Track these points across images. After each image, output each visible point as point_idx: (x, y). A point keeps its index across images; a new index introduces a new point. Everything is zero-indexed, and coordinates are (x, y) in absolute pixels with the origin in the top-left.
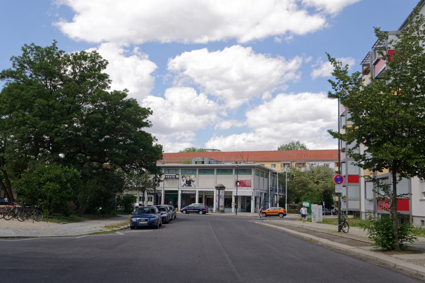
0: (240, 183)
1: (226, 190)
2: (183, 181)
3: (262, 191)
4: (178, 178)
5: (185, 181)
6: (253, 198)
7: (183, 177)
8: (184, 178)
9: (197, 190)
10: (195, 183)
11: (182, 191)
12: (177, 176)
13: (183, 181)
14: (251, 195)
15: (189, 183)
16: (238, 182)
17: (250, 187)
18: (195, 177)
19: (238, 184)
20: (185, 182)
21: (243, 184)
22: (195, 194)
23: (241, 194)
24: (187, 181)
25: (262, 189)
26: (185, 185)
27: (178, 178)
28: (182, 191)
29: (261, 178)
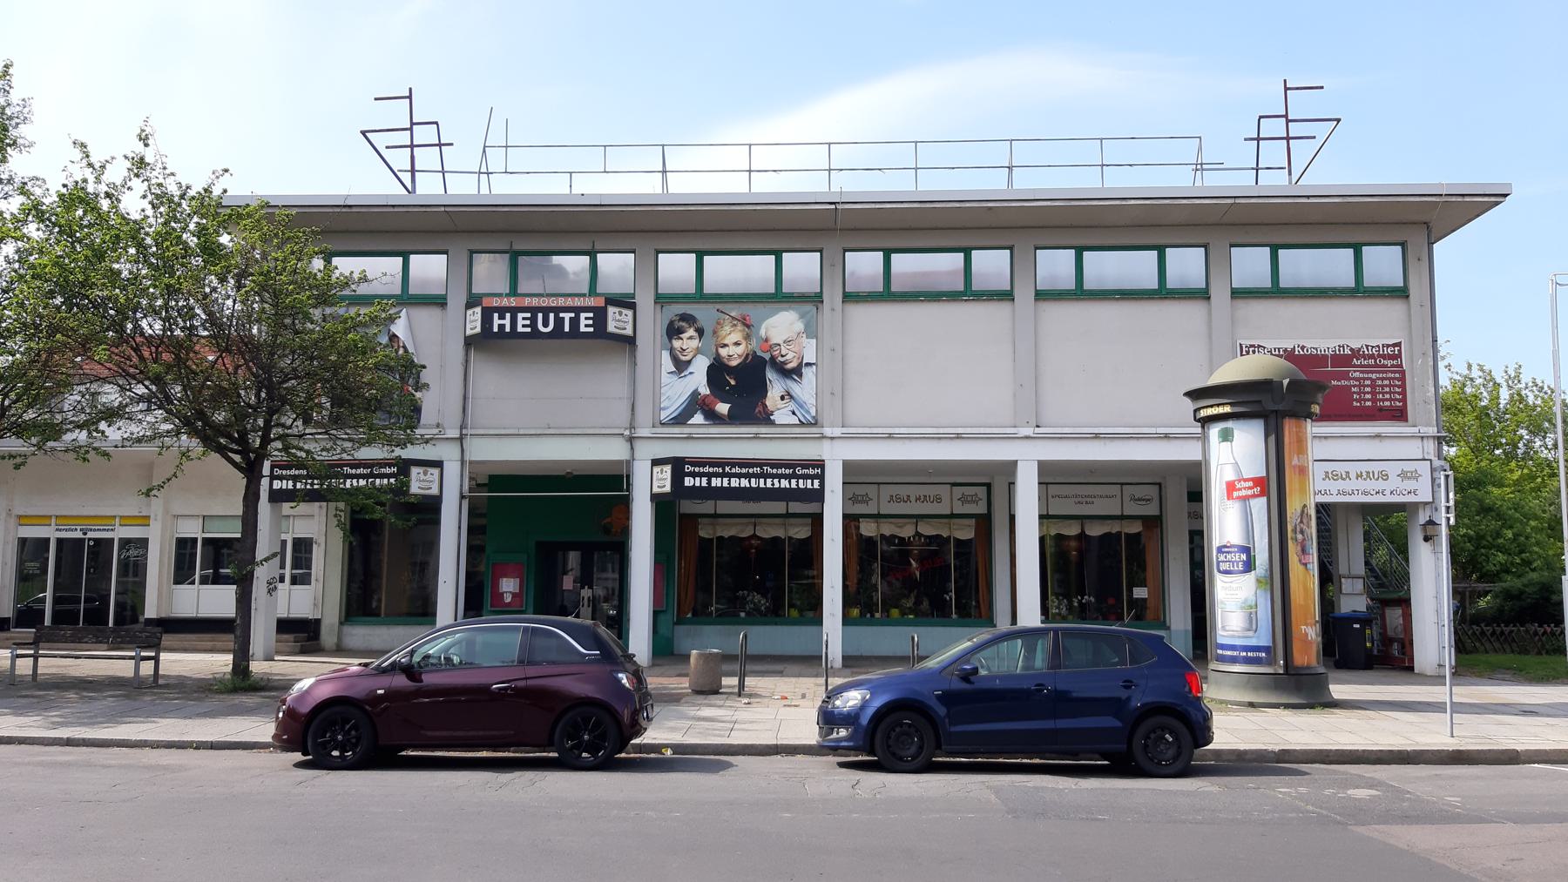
2: (681, 366)
4: (630, 341)
5: (701, 366)
7: (673, 332)
8: (688, 342)
9: (835, 457)
10: (805, 389)
13: (681, 366)
15: (742, 388)
17: (1399, 415)
18: (811, 331)
20: (697, 379)
22: (818, 496)
24: (717, 371)
26: (696, 403)
27: (630, 341)
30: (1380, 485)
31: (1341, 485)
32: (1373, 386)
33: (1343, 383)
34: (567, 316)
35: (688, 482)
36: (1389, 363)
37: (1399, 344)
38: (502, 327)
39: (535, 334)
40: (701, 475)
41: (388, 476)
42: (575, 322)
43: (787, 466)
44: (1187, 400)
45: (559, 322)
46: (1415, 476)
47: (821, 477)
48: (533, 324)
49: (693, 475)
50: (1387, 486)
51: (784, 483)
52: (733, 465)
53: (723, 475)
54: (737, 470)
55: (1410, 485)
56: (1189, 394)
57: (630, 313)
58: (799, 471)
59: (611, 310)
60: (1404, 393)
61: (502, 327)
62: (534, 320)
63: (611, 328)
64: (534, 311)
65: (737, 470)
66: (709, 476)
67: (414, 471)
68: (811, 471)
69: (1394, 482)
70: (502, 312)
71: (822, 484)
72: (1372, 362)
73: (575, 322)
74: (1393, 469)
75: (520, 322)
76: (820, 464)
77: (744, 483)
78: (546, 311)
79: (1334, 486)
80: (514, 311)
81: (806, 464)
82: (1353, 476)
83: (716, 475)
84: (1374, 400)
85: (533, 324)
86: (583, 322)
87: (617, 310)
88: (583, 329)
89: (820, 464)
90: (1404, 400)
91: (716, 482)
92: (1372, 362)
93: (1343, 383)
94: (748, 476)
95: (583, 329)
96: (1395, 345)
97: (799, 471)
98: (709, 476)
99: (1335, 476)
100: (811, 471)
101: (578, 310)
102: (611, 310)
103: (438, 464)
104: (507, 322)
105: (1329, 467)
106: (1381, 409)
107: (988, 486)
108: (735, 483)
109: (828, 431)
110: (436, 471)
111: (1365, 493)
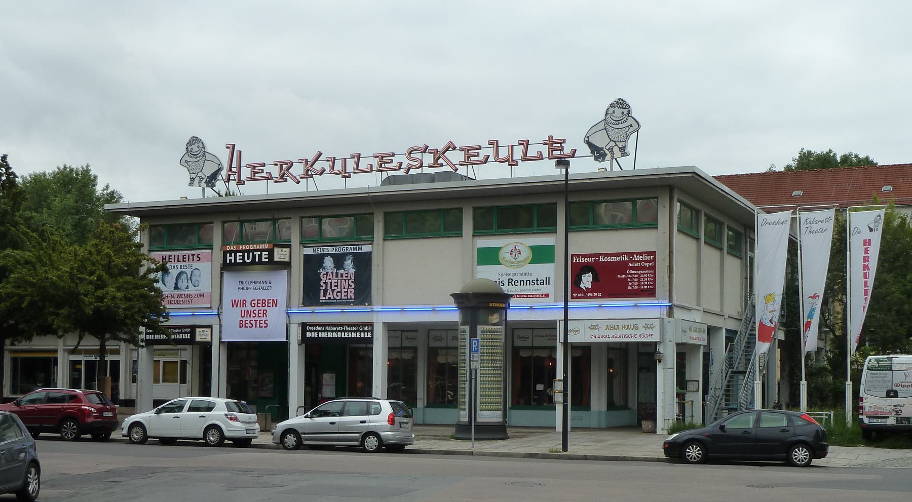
0: (595, 280)
1: (512, 316)
3: (715, 322)
6: (669, 354)
11: (304, 326)
12: (280, 255)
14: (656, 338)
16: (586, 268)
17: (651, 293)
19: (587, 280)
21: (611, 279)
22: (370, 341)
23: (602, 332)
25: (717, 309)
28: (304, 326)
29: (710, 255)
30: (633, 332)
31: (614, 332)
32: (639, 278)
33: (624, 276)
34: (257, 254)
35: (308, 335)
36: (647, 265)
37: (654, 253)
38: (230, 260)
39: (244, 263)
40: (314, 331)
41: (187, 333)
42: (260, 256)
43: (355, 326)
44: (452, 299)
45: (254, 256)
46: (652, 327)
47: (372, 331)
48: (243, 259)
49: (311, 331)
50: (638, 332)
51: (354, 335)
52: (329, 326)
53: (324, 331)
54: (331, 328)
55: (649, 332)
56: (452, 295)
57: (288, 250)
58: (361, 328)
59: (276, 250)
60: (655, 281)
61: (230, 260)
62: (243, 256)
63: (276, 258)
64: (243, 251)
65: (331, 328)
66: (318, 331)
67: (198, 330)
68: (367, 328)
69: (641, 330)
70: (230, 252)
71: (372, 335)
72: (638, 264)
73: (260, 256)
74: (641, 324)
75: (238, 258)
76: (371, 325)
77: (335, 335)
78: (248, 251)
79: (611, 333)
80: (235, 252)
81: (364, 325)
82: (620, 327)
83: (321, 331)
84: (639, 286)
85: (243, 259)
86: (264, 256)
87: (280, 249)
88: (264, 260)
89: (371, 325)
90: (654, 285)
91: (321, 335)
92: (638, 264)
93: (624, 276)
94: (336, 331)
95: (264, 260)
96: (649, 253)
97: (361, 328)
98: (318, 331)
99: (613, 328)
100: (367, 328)
101: (261, 251)
102: (276, 250)
103: (210, 327)
104: (233, 258)
105: (609, 323)
106: (643, 290)
107: (513, 330)
108: (330, 335)
109: (376, 308)
110: (209, 330)
111: (626, 337)
